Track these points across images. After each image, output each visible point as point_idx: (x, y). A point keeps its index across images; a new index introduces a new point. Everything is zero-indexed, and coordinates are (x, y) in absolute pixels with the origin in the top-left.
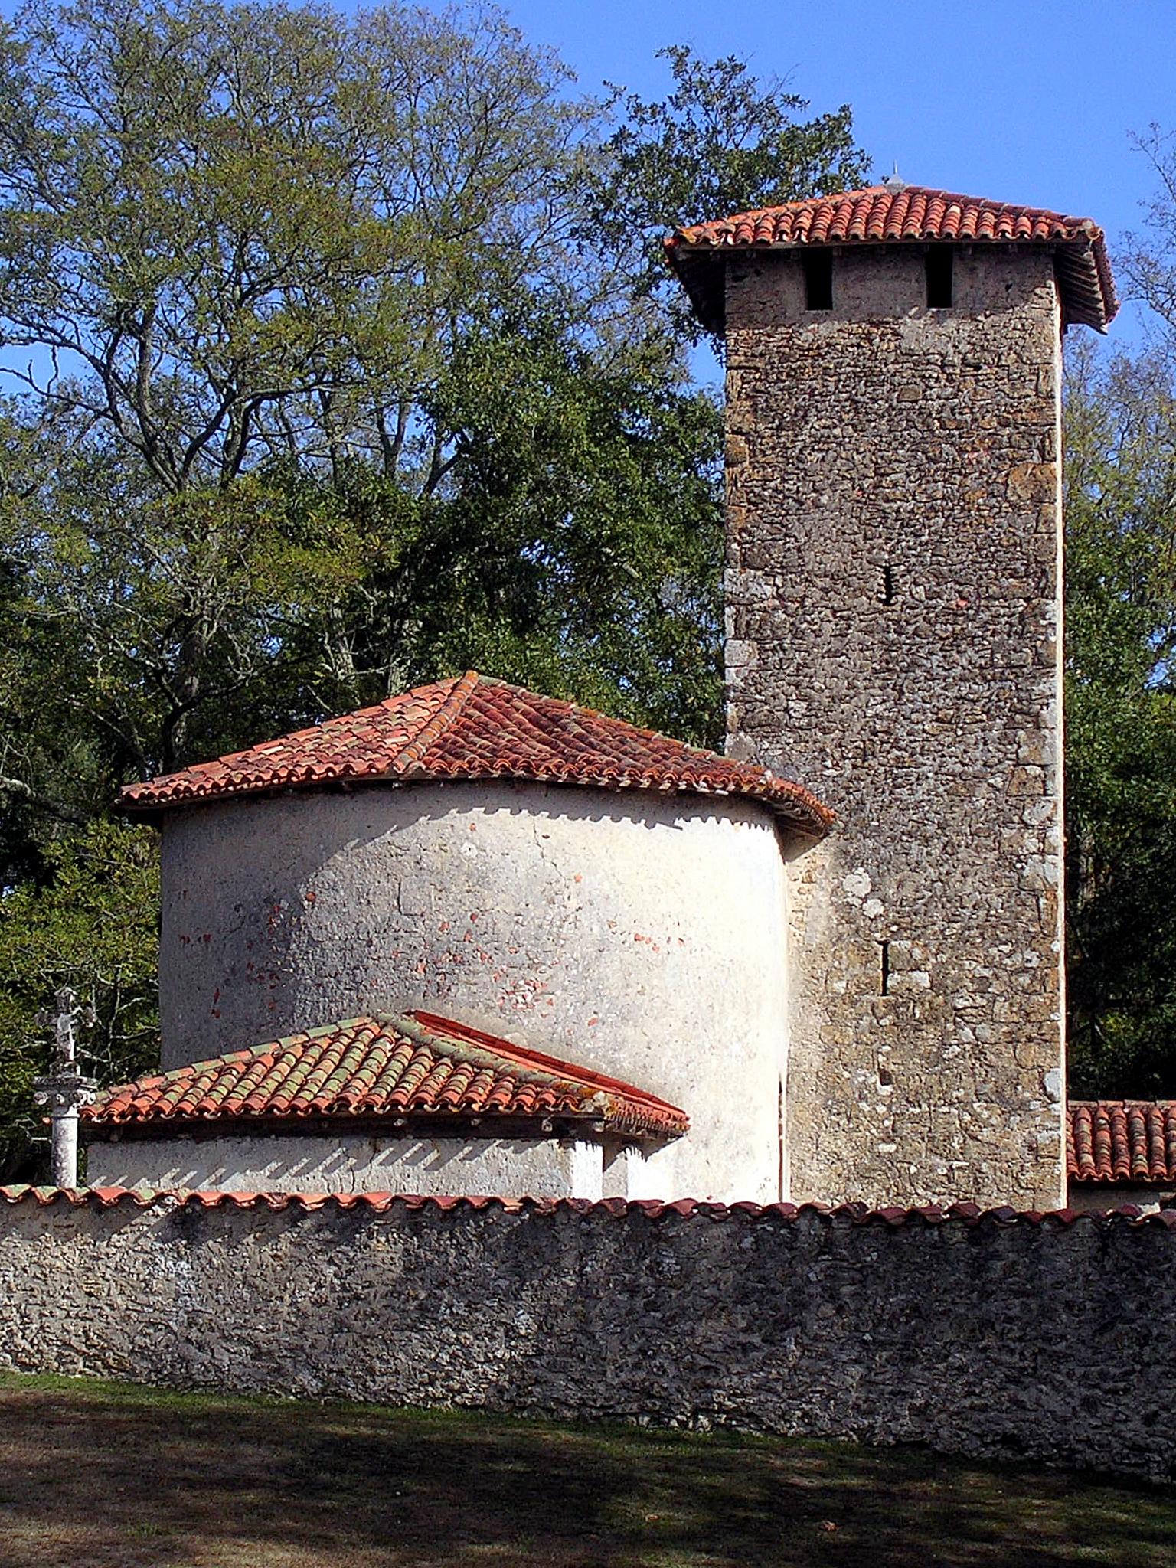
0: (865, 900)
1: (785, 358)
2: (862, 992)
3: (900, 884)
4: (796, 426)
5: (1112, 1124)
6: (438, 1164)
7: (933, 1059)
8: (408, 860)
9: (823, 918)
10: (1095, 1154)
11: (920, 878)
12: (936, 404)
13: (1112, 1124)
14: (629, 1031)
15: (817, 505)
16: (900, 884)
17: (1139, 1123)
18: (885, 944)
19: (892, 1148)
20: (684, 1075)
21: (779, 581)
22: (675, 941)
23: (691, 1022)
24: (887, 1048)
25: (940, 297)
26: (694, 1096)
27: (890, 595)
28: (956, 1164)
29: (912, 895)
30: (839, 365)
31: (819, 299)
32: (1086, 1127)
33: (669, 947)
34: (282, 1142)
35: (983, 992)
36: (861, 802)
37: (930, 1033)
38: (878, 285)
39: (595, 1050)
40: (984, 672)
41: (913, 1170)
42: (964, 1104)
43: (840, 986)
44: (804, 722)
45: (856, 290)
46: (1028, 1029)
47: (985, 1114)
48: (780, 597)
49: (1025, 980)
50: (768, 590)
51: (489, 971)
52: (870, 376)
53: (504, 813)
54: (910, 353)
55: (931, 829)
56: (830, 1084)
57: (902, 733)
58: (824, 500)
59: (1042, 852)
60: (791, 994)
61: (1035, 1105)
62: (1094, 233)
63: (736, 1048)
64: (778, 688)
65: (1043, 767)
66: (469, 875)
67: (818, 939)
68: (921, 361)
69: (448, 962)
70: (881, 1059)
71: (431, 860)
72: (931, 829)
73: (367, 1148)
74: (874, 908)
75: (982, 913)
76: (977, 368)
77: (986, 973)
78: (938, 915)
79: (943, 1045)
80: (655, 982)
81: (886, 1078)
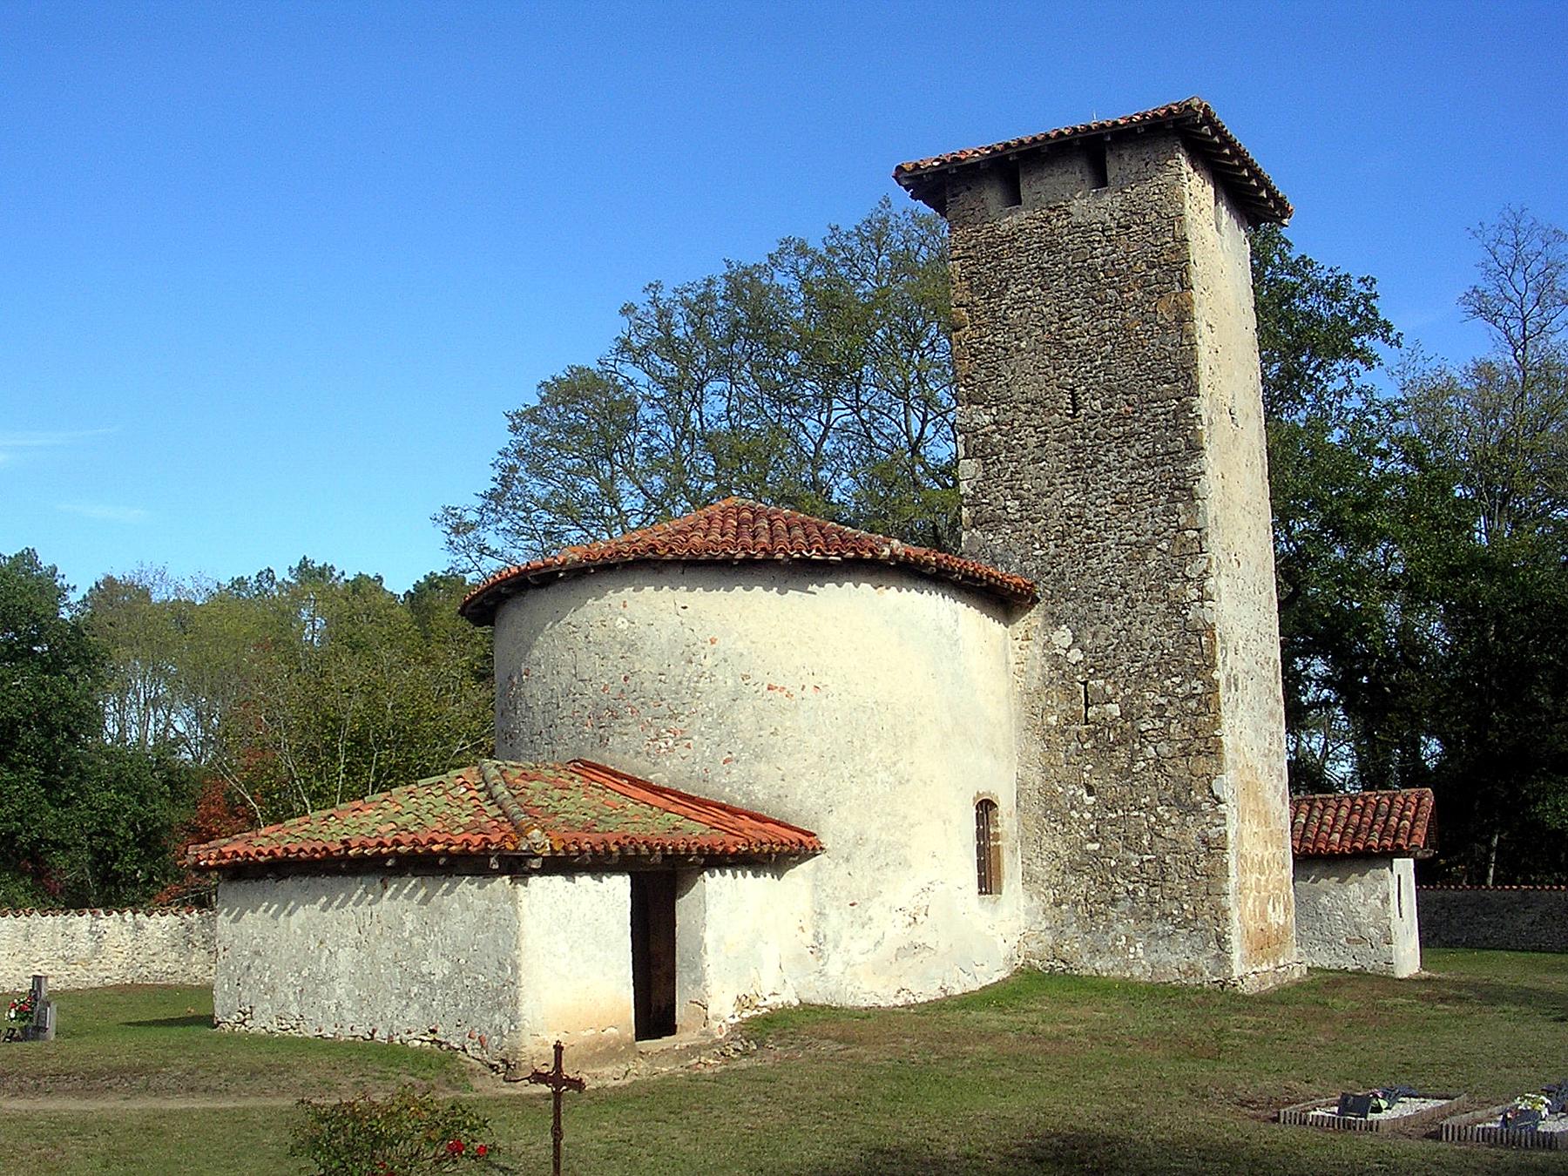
0: (1068, 650)
1: (989, 245)
2: (1069, 723)
3: (1095, 635)
4: (1000, 294)
5: (1363, 809)
6: (426, 900)
7: (1125, 773)
8: (580, 636)
9: (1038, 667)
10: (1343, 834)
11: (1108, 629)
12: (1100, 261)
13: (1363, 809)
14: (763, 767)
15: (1018, 350)
16: (1095, 635)
17: (1384, 807)
18: (1085, 683)
19: (1097, 846)
20: (821, 802)
21: (994, 411)
22: (810, 688)
23: (828, 755)
24: (1089, 767)
25: (1101, 181)
26: (832, 819)
27: (1075, 410)
28: (1146, 857)
29: (1104, 643)
30: (1028, 244)
31: (1014, 199)
32: (1343, 812)
33: (804, 694)
34: (326, 880)
35: (1161, 717)
36: (1063, 573)
37: (1121, 752)
38: (1052, 180)
39: (730, 785)
40: (1149, 461)
41: (1113, 863)
42: (1150, 809)
43: (1052, 720)
44: (1017, 516)
45: (1037, 187)
46: (1198, 744)
47: (1167, 816)
48: (996, 422)
49: (1193, 704)
50: (987, 418)
51: (637, 723)
52: (1050, 247)
53: (649, 590)
54: (1079, 225)
55: (1116, 589)
56: (1049, 798)
57: (1090, 516)
58: (1023, 345)
59: (1201, 599)
60: (1017, 728)
61: (1205, 806)
62: (1199, 106)
63: (882, 775)
64: (998, 492)
65: (1199, 530)
66: (622, 644)
67: (1035, 683)
68: (1086, 230)
69: (608, 716)
70: (1086, 775)
71: (597, 634)
72: (1116, 589)
73: (379, 886)
74: (1076, 655)
75: (1158, 653)
76: (1128, 228)
77: (1163, 701)
78: (1124, 657)
79: (1133, 762)
80: (788, 724)
81: (1090, 790)
